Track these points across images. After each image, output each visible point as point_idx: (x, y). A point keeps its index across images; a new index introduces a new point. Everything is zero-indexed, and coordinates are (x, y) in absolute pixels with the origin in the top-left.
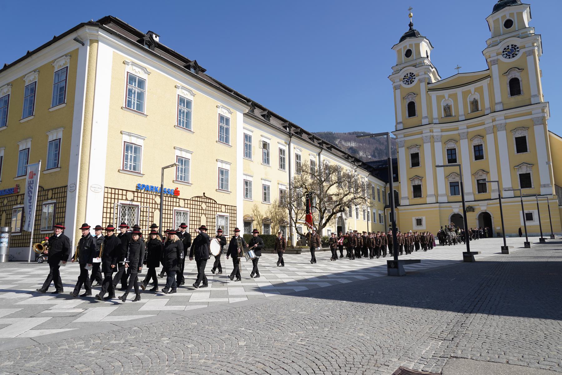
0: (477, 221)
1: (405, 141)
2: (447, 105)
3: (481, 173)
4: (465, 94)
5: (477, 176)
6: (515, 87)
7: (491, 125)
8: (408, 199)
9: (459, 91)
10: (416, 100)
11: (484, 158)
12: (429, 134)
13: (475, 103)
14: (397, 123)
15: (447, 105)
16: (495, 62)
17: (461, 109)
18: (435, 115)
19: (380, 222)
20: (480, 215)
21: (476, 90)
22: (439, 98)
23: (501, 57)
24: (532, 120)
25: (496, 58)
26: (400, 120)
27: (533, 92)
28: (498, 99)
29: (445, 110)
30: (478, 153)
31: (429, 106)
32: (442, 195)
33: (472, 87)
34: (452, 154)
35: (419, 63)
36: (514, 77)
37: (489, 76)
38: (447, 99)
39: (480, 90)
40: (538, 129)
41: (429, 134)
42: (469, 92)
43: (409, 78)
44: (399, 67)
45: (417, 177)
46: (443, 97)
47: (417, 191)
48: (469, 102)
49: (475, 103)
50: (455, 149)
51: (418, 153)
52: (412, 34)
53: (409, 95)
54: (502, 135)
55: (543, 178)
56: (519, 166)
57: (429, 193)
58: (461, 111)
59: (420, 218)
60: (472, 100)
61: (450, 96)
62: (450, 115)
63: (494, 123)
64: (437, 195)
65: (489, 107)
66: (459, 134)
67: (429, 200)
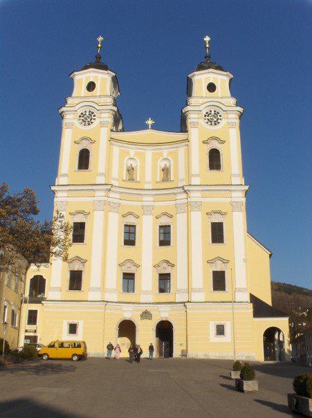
3: (165, 265)
6: (215, 159)
10: (91, 148)
11: (172, 244)
25: (197, 120)
28: (195, 169)
34: (129, 233)
47: (76, 280)
48: (159, 167)
49: (166, 171)
50: (134, 226)
53: (83, 139)
58: (148, 177)
59: (74, 322)
60: (163, 166)
62: (132, 180)
64: (102, 289)
66: (143, 207)
67: (92, 296)
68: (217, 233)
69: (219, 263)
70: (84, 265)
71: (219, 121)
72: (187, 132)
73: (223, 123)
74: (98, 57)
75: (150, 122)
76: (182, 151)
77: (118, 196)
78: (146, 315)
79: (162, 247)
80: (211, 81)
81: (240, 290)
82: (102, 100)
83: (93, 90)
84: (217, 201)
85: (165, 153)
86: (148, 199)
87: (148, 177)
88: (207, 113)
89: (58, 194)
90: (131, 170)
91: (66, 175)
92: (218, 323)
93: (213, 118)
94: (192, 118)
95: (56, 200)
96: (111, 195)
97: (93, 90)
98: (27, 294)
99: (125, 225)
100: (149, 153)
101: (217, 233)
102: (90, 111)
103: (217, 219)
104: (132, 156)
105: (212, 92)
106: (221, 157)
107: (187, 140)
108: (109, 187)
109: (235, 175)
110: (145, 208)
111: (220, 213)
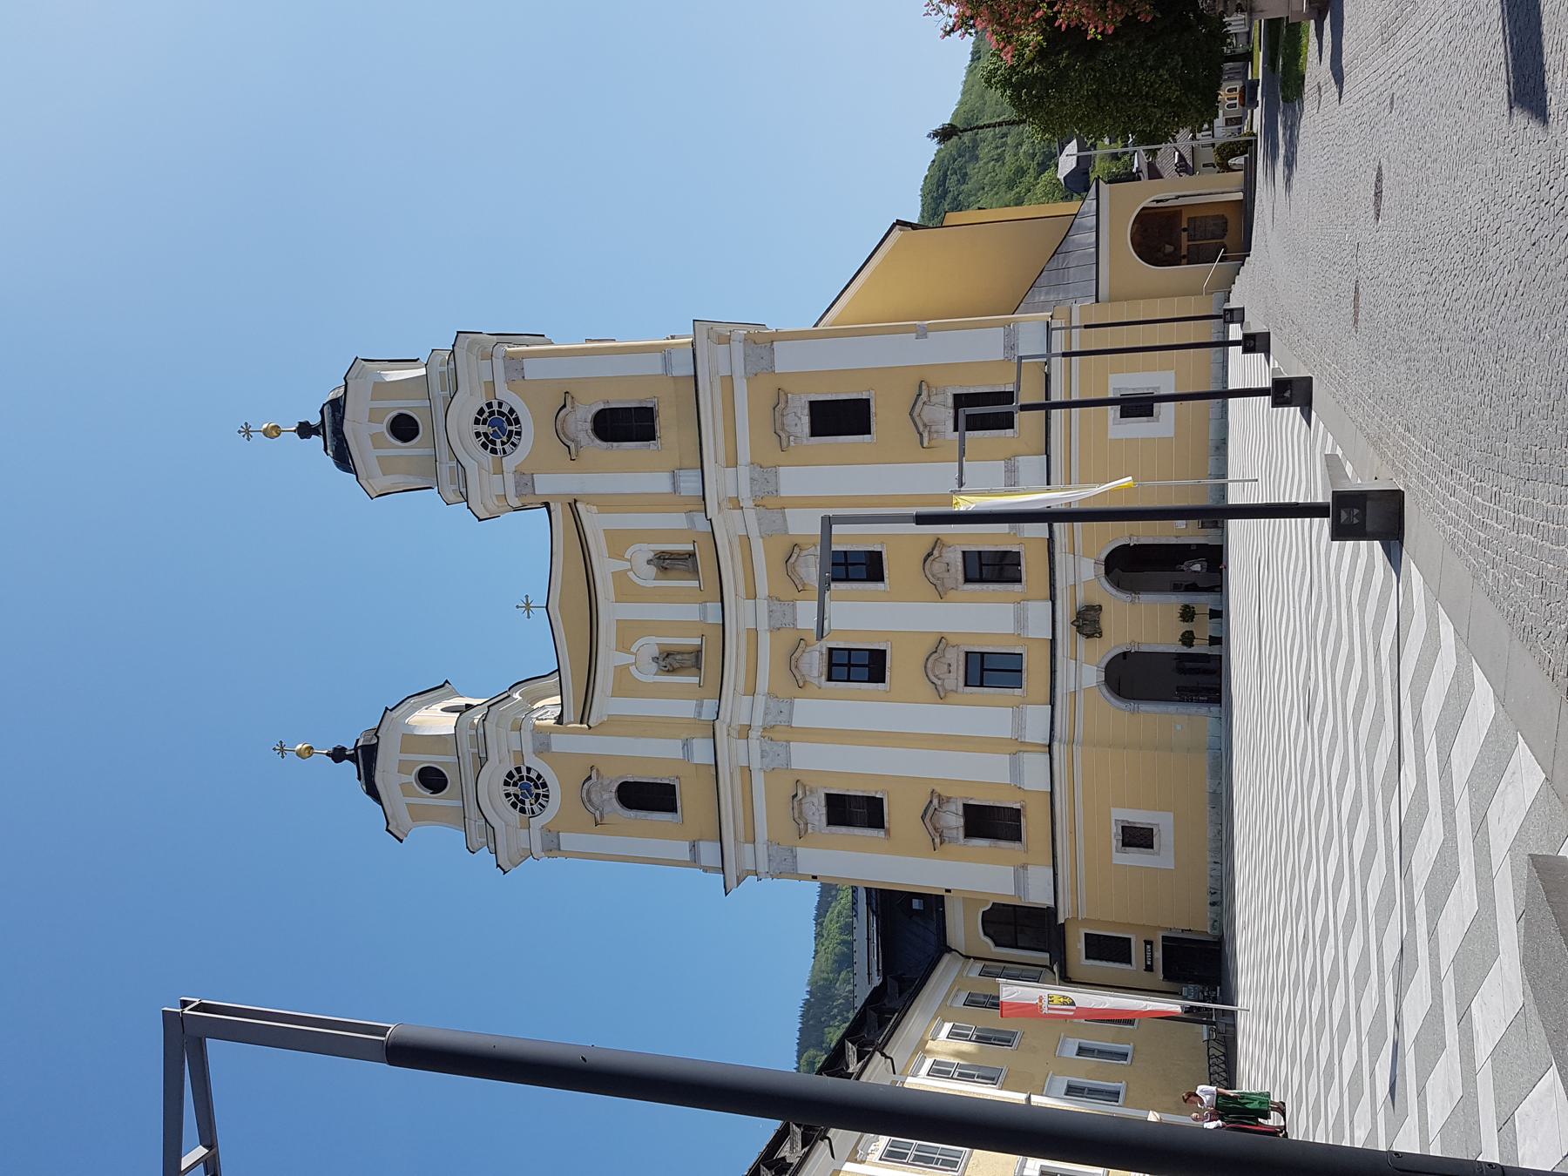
0: (1145, 598)
1: (770, 842)
2: (655, 659)
3: (937, 567)
4: (627, 591)
5: (949, 583)
6: (625, 425)
7: (751, 515)
8: (1024, 867)
9: (611, 612)
12: (755, 744)
13: (666, 562)
14: (694, 861)
15: (655, 659)
16: (525, 481)
17: (678, 613)
18: (684, 709)
20: (1118, 585)
21: (616, 553)
22: (625, 685)
23: (511, 462)
24: (752, 377)
25: (510, 479)
26: (682, 850)
27: (653, 365)
28: (659, 483)
29: (671, 671)
31: (647, 727)
32: (1019, 724)
33: (604, 568)
34: (849, 665)
35: (474, 742)
36: (589, 426)
37: (573, 507)
38: (632, 659)
39: (618, 542)
40: (787, 360)
41: (755, 744)
42: (619, 576)
43: (526, 789)
44: (475, 823)
45: (931, 812)
46: (621, 671)
47: (990, 823)
49: (666, 562)
50: (831, 650)
51: (828, 796)
52: (366, 757)
53: (587, 801)
54: (794, 480)
55: (976, 353)
56: (922, 430)
57: (1006, 779)
58: (688, 612)
59: (1115, 830)
60: (653, 570)
61: (623, 646)
63: (747, 503)
64: (1016, 747)
66: (774, 630)
67: (1035, 775)
69: (928, 414)
70: (949, 799)
71: (505, 410)
78: (1088, 622)
87: (688, 612)
91: (693, 847)
98: (1044, 957)
99: (830, 679)
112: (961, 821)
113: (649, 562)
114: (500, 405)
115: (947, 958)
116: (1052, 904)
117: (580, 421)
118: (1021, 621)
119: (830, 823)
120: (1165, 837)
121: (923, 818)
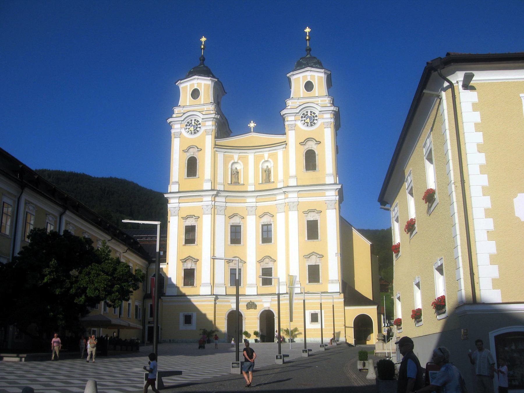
6: (310, 160)
10: (198, 156)
19: (136, 317)
25: (293, 123)
30: (267, 235)
32: (219, 285)
34: (236, 232)
49: (267, 173)
53: (190, 147)
54: (294, 216)
58: (251, 179)
60: (265, 167)
62: (237, 183)
65: (282, 179)
68: (313, 230)
70: (196, 264)
72: (285, 134)
73: (319, 123)
74: (203, 59)
75: (252, 125)
76: (280, 152)
77: (223, 200)
78: (251, 306)
79: (265, 244)
80: (309, 80)
81: (332, 282)
82: (205, 108)
83: (195, 97)
84: (311, 200)
85: (266, 155)
86: (251, 201)
87: (251, 179)
88: (304, 114)
89: (171, 201)
90: (235, 174)
92: (313, 311)
93: (310, 119)
94: (290, 120)
95: (169, 206)
96: (217, 199)
97: (195, 97)
99: (231, 226)
100: (251, 156)
101: (313, 230)
102: (195, 120)
103: (311, 217)
104: (236, 161)
105: (309, 91)
106: (317, 157)
107: (285, 143)
108: (215, 193)
109: (329, 175)
110: (249, 208)
111: (313, 211)
112: (189, 268)
113: (267, 166)
114: (316, 120)
115: (147, 263)
116: (167, 294)
117: (311, 145)
118: (251, 286)
119: (186, 226)
120: (188, 327)
121: (189, 256)
